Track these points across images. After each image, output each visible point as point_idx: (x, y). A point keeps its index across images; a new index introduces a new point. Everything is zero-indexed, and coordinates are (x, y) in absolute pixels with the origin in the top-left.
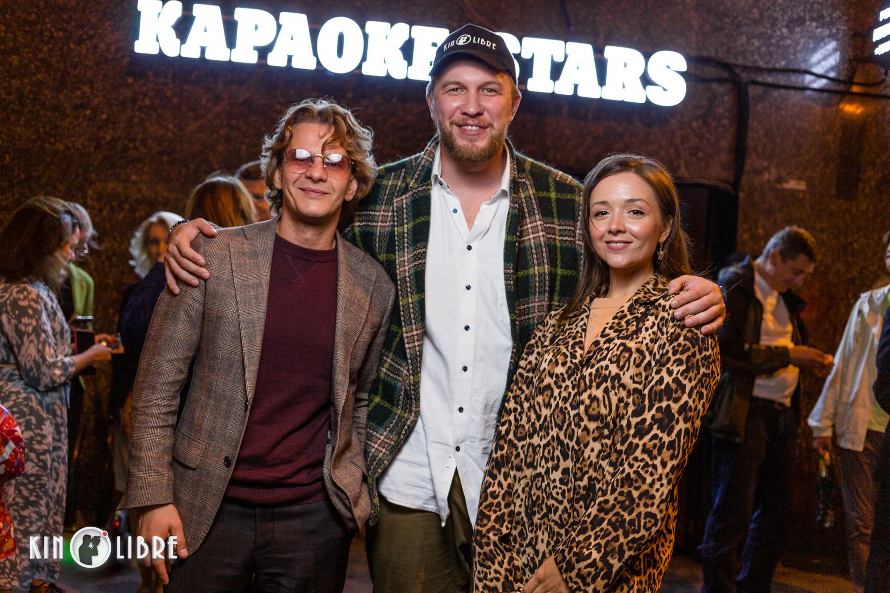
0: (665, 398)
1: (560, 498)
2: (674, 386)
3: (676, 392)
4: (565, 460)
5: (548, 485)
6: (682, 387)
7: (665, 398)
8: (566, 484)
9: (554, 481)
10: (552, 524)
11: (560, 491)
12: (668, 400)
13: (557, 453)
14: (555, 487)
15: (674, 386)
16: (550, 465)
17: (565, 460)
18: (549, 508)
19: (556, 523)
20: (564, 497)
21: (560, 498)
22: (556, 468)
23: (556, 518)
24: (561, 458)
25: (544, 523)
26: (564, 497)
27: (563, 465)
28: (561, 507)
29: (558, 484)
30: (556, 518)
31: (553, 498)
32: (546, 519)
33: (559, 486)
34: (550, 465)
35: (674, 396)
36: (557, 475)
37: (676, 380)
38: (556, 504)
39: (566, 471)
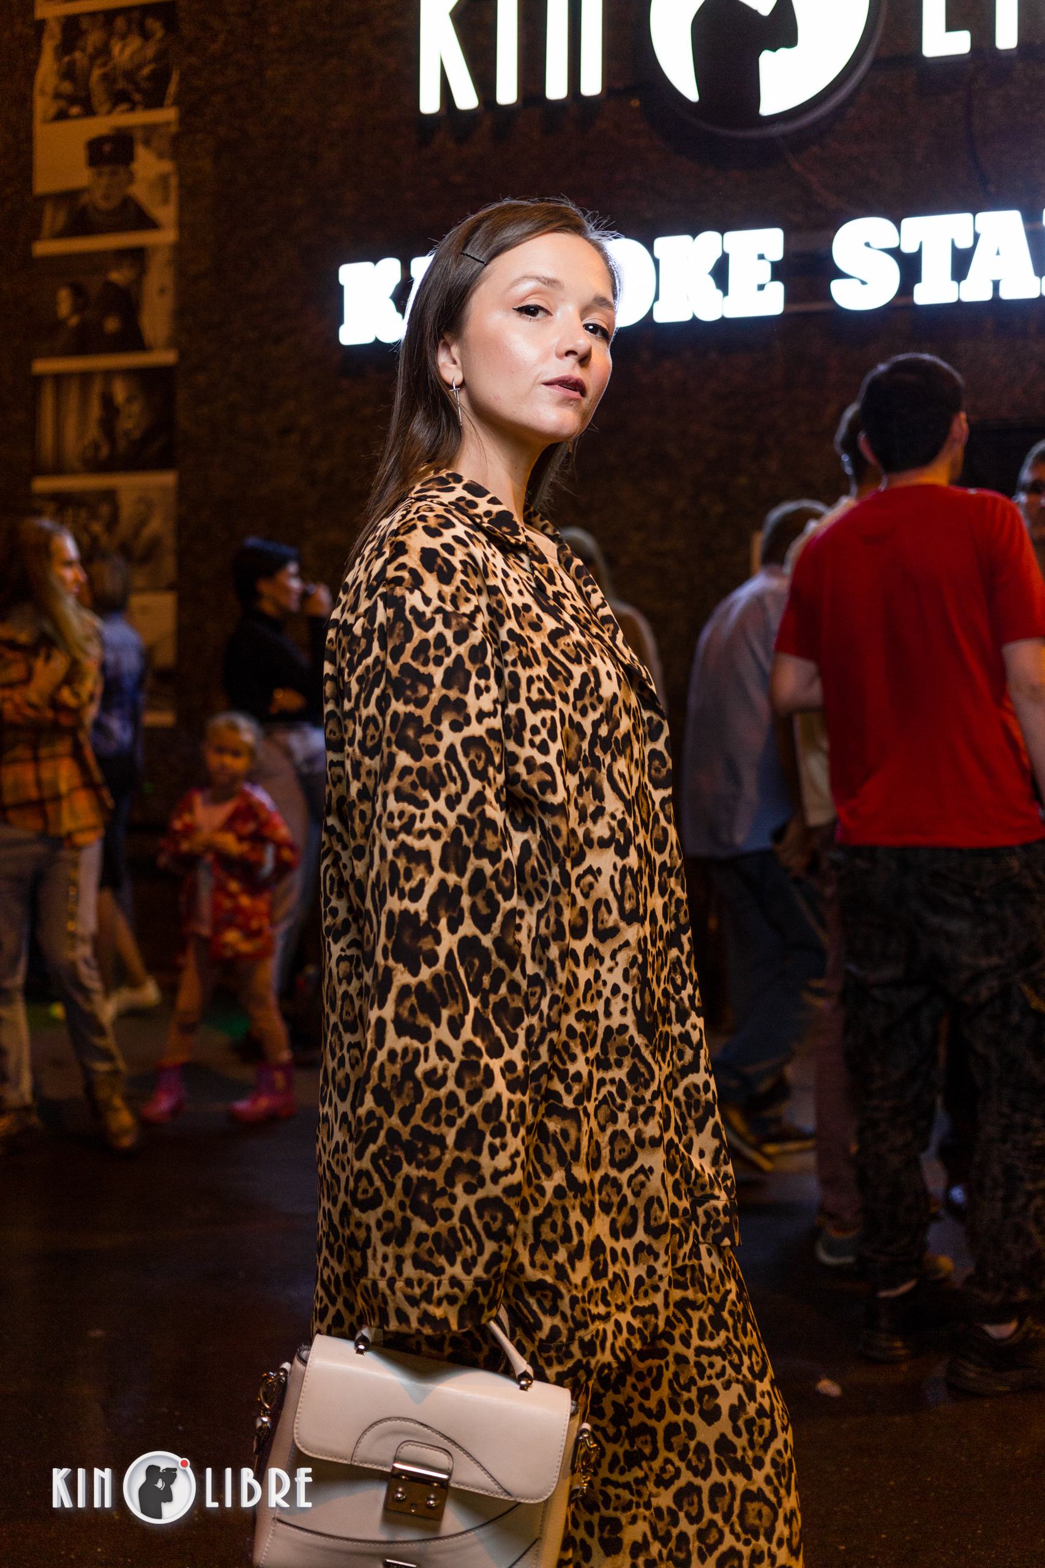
0: (429, 987)
1: (704, 1360)
2: (423, 1020)
3: (412, 1011)
4: (723, 1436)
5: (737, 1368)
6: (403, 1027)
7: (429, 987)
8: (702, 1392)
9: (727, 1386)
10: (701, 1297)
11: (709, 1372)
12: (421, 984)
13: (741, 1442)
14: (719, 1375)
15: (423, 1020)
16: (751, 1409)
17: (723, 1436)
18: (718, 1323)
19: (696, 1307)
20: (698, 1365)
21: (704, 1360)
22: (736, 1411)
23: (696, 1316)
24: (731, 1436)
25: (718, 1289)
26: (698, 1365)
27: (724, 1425)
28: (695, 1341)
29: (718, 1384)
30: (696, 1316)
31: (718, 1351)
32: (717, 1298)
33: (714, 1382)
34: (751, 1409)
35: (413, 1000)
36: (726, 1400)
37: (423, 1035)
38: (707, 1343)
39: (711, 1416)
